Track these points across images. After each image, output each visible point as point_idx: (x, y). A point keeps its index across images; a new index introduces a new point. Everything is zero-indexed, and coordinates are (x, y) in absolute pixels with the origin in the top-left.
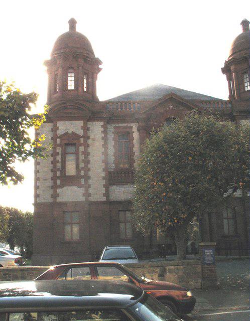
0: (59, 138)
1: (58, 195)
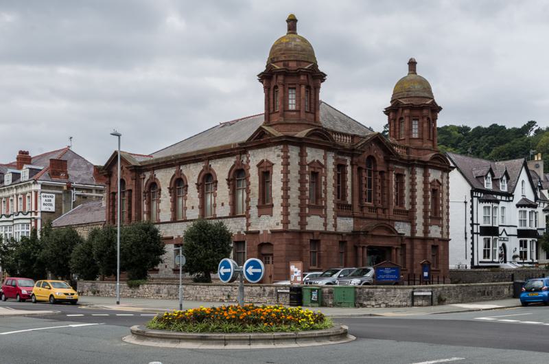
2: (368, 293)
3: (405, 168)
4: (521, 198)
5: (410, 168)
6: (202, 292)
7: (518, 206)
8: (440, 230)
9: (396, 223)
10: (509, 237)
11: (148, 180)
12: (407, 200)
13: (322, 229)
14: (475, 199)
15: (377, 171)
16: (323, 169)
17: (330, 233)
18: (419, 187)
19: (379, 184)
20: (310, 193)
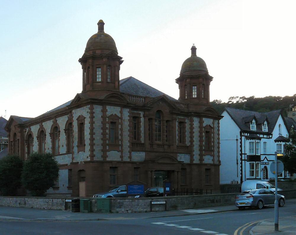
0: (107, 117)
2: (119, 203)
3: (186, 118)
4: (278, 136)
5: (190, 118)
6: (35, 202)
7: (276, 141)
8: (212, 158)
9: (178, 154)
11: (28, 133)
12: (187, 139)
13: (120, 160)
14: (243, 138)
15: (164, 120)
16: (120, 120)
17: (125, 162)
18: (196, 130)
19: (166, 129)
20: (109, 136)
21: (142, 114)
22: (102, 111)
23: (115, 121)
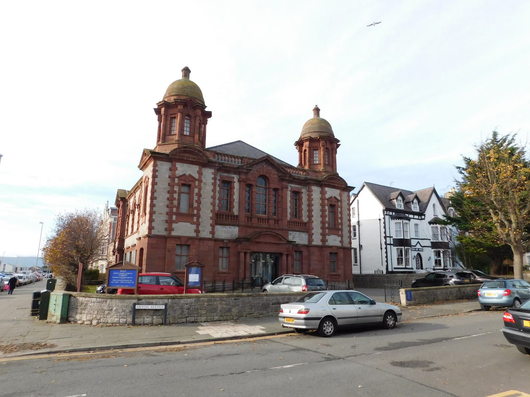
0: (177, 177)
1: (173, 230)
4: (433, 217)
7: (430, 223)
8: (339, 239)
9: (290, 232)
10: (423, 248)
13: (194, 235)
21: (236, 178)
22: (170, 169)
23: (190, 183)
